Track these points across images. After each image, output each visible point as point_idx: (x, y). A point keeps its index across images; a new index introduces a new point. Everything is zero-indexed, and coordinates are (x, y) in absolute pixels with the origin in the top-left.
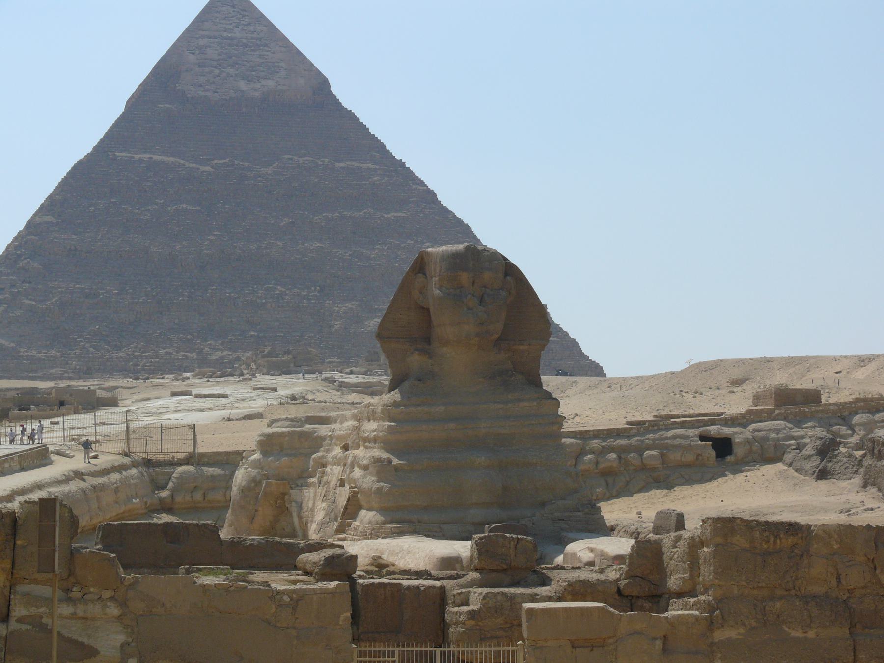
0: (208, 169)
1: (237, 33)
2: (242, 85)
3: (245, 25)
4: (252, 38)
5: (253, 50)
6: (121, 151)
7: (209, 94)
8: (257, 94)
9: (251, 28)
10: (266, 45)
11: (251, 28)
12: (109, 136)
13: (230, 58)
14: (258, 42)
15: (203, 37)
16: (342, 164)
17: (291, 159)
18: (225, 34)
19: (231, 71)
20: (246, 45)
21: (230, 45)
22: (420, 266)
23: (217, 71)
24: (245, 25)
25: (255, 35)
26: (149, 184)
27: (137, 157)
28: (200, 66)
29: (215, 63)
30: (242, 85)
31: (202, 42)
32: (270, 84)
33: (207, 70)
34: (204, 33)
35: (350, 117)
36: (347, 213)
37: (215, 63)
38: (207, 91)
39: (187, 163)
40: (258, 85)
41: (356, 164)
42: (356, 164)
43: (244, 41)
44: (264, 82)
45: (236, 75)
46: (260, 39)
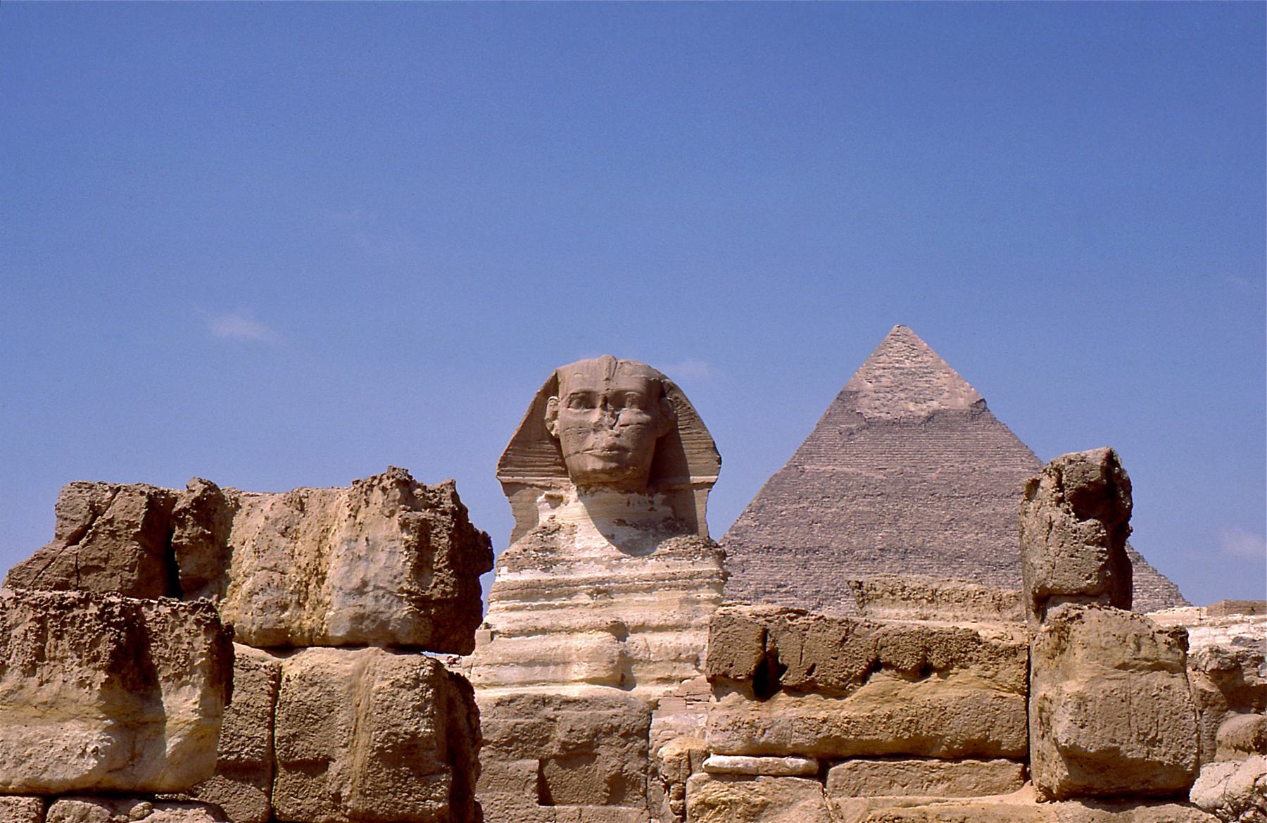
0: (881, 477)
1: (907, 363)
2: (911, 406)
3: (915, 357)
4: (920, 367)
5: (922, 377)
6: (809, 465)
7: (882, 415)
8: (923, 414)
9: (919, 359)
10: (932, 373)
11: (919, 359)
12: (800, 453)
13: (901, 384)
14: (925, 370)
15: (878, 369)
16: (996, 469)
17: (952, 466)
18: (897, 365)
19: (902, 395)
20: (914, 373)
21: (901, 374)
22: (552, 387)
23: (890, 396)
24: (915, 357)
25: (923, 365)
26: (833, 491)
27: (823, 469)
28: (875, 392)
29: (888, 389)
30: (911, 406)
31: (877, 373)
32: (935, 404)
33: (881, 395)
34: (882, 365)
35: (1005, 430)
36: (1000, 509)
37: (888, 389)
38: (881, 412)
39: (864, 472)
40: (924, 406)
41: (1009, 469)
42: (1009, 469)
43: (913, 370)
44: (929, 403)
45: (906, 398)
46: (926, 368)
